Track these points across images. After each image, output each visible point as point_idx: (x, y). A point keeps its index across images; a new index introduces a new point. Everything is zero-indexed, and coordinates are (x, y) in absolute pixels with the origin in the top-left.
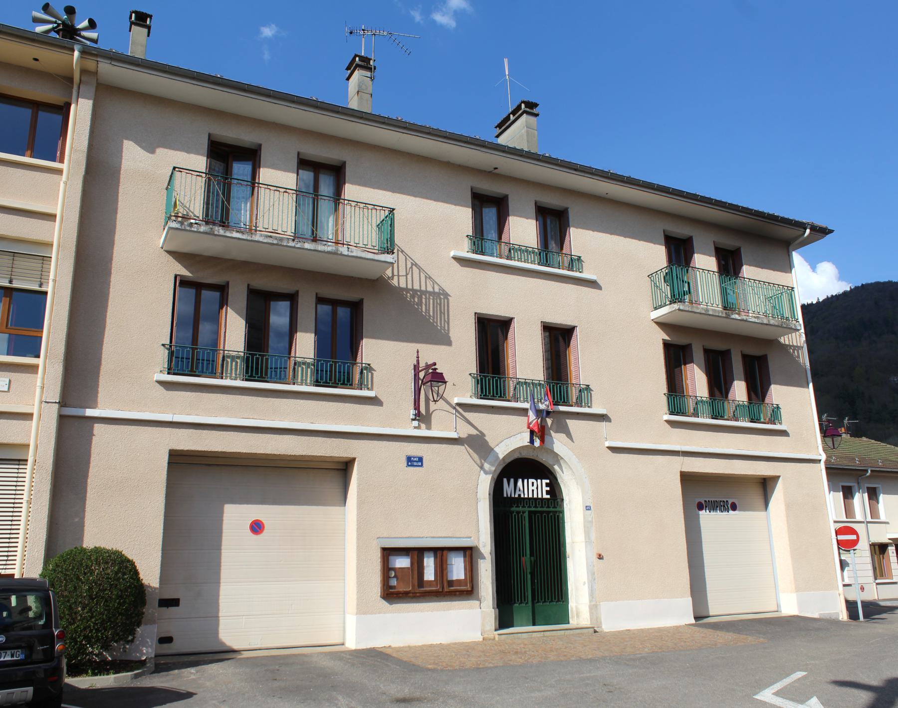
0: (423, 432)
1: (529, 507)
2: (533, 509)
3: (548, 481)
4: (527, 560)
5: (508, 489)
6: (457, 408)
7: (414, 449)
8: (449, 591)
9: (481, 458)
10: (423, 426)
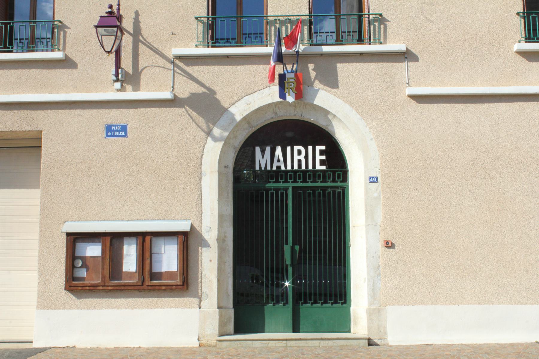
0: (130, 95)
1: (295, 181)
2: (299, 184)
3: (323, 148)
4: (287, 249)
5: (262, 160)
6: (177, 62)
7: (115, 116)
8: (149, 283)
9: (207, 121)
10: (129, 87)
